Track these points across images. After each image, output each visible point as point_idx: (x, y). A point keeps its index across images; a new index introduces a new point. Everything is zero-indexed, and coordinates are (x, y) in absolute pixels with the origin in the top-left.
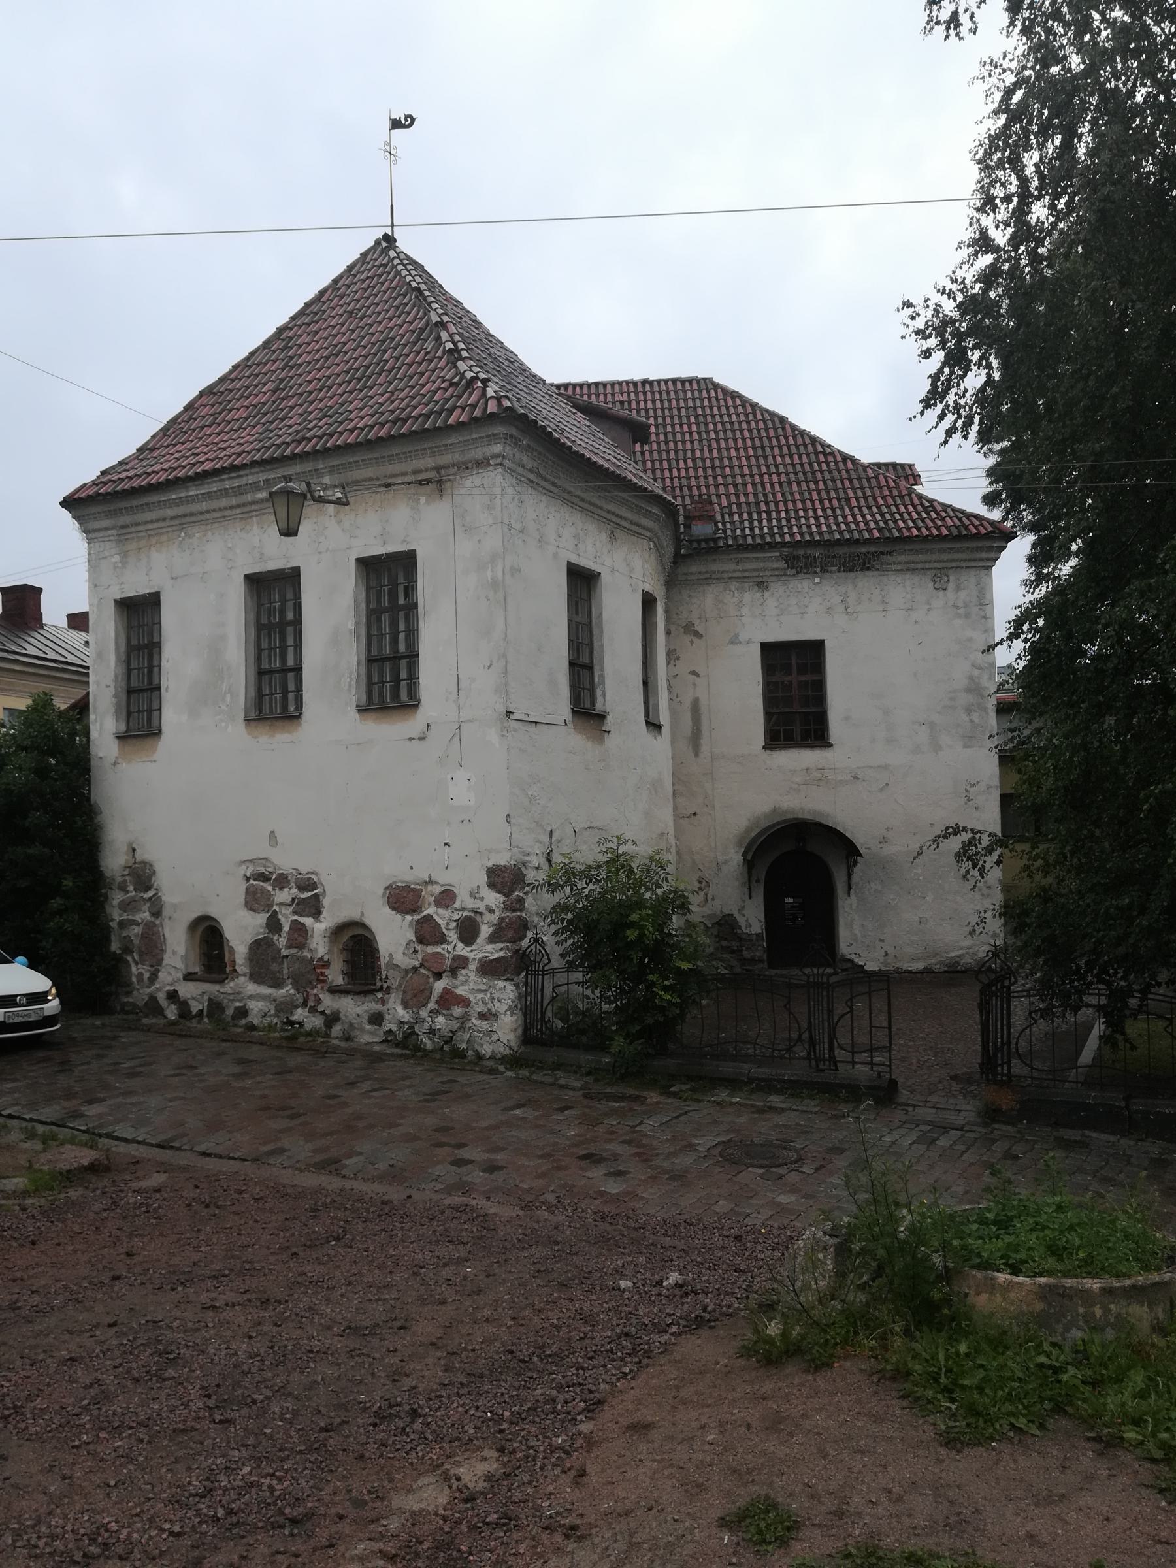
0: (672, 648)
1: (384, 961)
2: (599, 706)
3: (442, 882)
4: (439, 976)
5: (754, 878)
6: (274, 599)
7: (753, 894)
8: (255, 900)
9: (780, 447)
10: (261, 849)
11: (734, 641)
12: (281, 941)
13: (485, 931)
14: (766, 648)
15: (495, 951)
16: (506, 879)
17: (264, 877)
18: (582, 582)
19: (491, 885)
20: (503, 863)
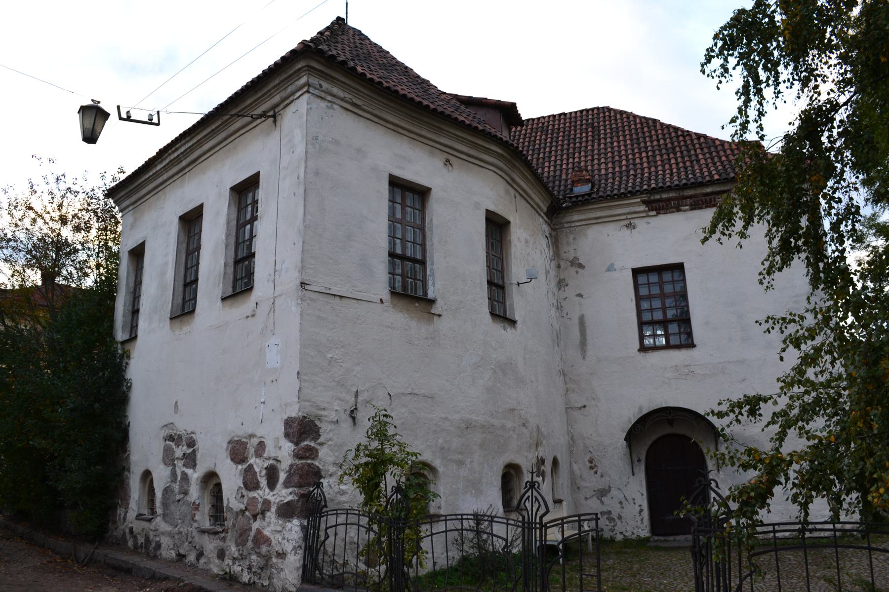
0: (562, 277)
2: (430, 295)
3: (258, 435)
5: (635, 459)
7: (636, 471)
8: (168, 458)
9: (651, 137)
11: (611, 268)
12: (176, 487)
13: (282, 476)
14: (637, 272)
16: (303, 430)
20: (294, 415)
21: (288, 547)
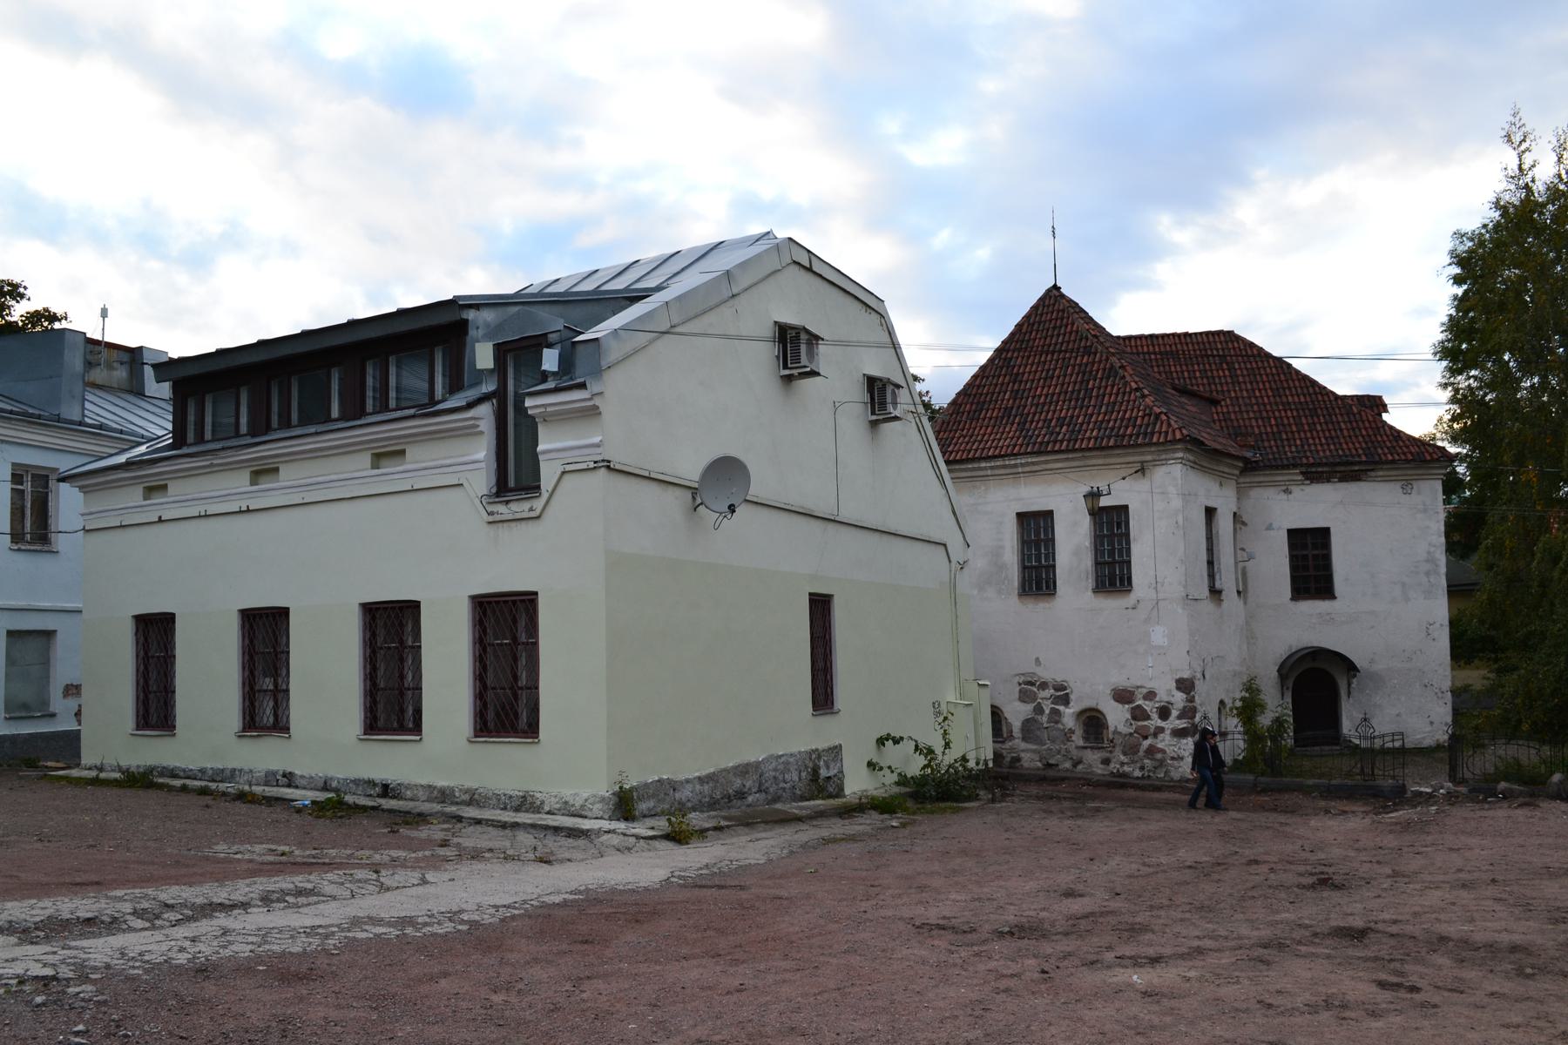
1: (1111, 729)
4: (1146, 738)
6: (1036, 529)
10: (1029, 667)
11: (1269, 527)
13: (1175, 713)
14: (1290, 532)
15: (1182, 724)
17: (1032, 684)
18: (1210, 512)
19: (1178, 688)
21: (1182, 753)
